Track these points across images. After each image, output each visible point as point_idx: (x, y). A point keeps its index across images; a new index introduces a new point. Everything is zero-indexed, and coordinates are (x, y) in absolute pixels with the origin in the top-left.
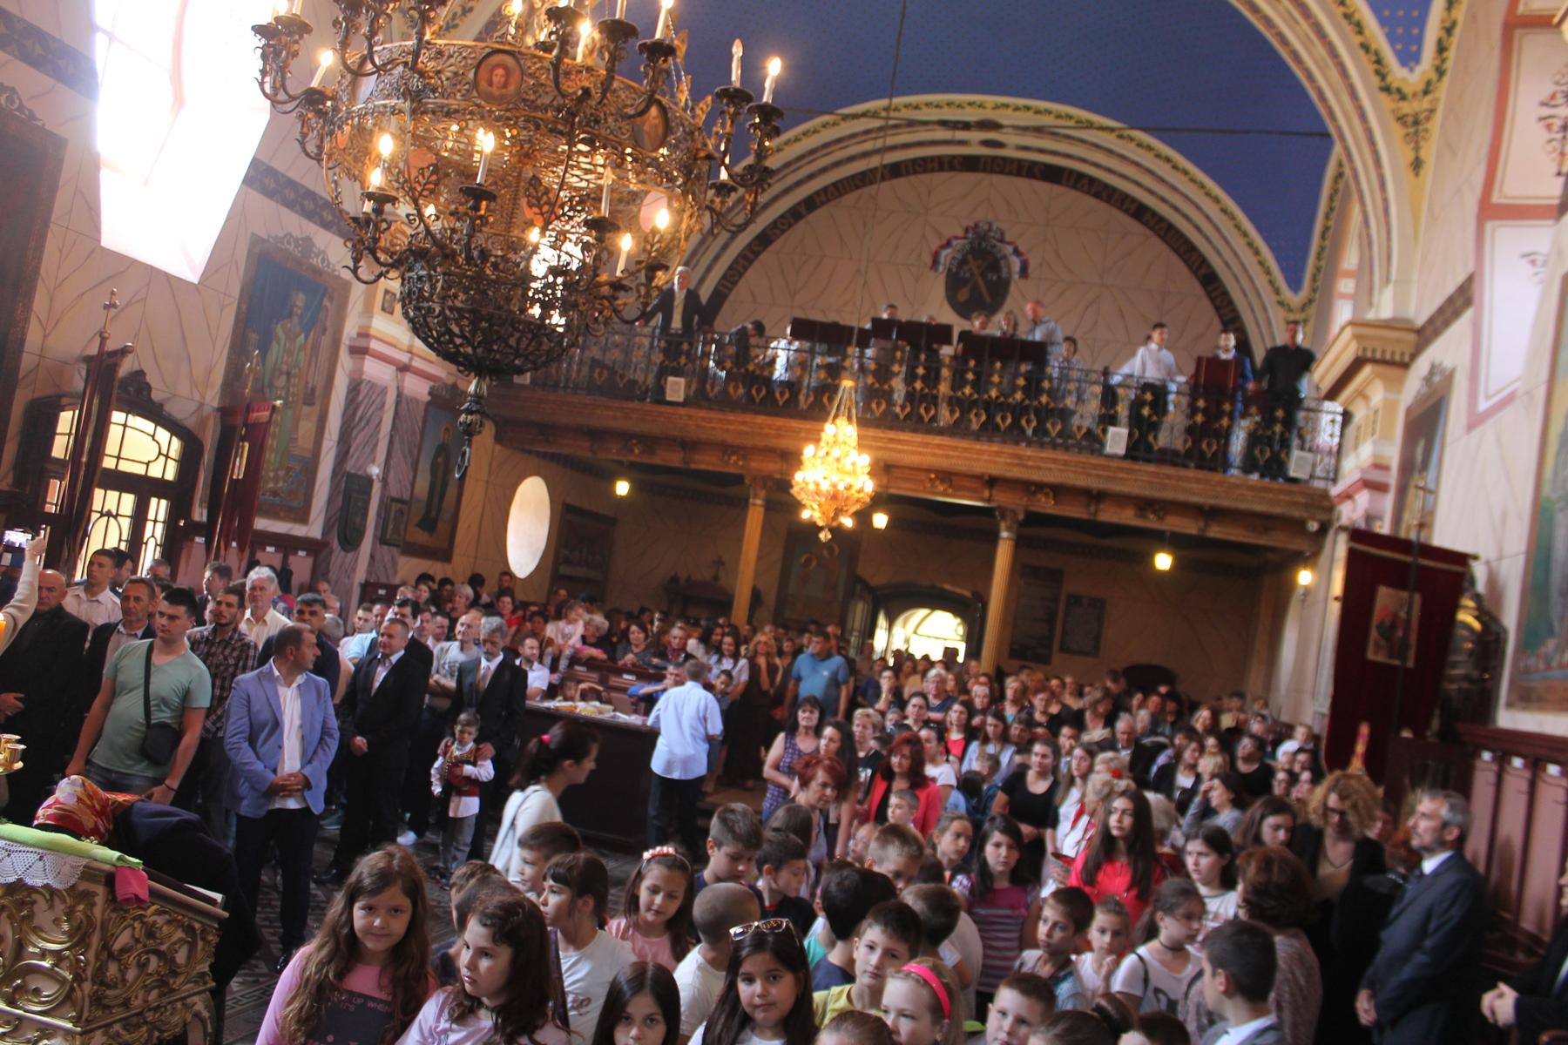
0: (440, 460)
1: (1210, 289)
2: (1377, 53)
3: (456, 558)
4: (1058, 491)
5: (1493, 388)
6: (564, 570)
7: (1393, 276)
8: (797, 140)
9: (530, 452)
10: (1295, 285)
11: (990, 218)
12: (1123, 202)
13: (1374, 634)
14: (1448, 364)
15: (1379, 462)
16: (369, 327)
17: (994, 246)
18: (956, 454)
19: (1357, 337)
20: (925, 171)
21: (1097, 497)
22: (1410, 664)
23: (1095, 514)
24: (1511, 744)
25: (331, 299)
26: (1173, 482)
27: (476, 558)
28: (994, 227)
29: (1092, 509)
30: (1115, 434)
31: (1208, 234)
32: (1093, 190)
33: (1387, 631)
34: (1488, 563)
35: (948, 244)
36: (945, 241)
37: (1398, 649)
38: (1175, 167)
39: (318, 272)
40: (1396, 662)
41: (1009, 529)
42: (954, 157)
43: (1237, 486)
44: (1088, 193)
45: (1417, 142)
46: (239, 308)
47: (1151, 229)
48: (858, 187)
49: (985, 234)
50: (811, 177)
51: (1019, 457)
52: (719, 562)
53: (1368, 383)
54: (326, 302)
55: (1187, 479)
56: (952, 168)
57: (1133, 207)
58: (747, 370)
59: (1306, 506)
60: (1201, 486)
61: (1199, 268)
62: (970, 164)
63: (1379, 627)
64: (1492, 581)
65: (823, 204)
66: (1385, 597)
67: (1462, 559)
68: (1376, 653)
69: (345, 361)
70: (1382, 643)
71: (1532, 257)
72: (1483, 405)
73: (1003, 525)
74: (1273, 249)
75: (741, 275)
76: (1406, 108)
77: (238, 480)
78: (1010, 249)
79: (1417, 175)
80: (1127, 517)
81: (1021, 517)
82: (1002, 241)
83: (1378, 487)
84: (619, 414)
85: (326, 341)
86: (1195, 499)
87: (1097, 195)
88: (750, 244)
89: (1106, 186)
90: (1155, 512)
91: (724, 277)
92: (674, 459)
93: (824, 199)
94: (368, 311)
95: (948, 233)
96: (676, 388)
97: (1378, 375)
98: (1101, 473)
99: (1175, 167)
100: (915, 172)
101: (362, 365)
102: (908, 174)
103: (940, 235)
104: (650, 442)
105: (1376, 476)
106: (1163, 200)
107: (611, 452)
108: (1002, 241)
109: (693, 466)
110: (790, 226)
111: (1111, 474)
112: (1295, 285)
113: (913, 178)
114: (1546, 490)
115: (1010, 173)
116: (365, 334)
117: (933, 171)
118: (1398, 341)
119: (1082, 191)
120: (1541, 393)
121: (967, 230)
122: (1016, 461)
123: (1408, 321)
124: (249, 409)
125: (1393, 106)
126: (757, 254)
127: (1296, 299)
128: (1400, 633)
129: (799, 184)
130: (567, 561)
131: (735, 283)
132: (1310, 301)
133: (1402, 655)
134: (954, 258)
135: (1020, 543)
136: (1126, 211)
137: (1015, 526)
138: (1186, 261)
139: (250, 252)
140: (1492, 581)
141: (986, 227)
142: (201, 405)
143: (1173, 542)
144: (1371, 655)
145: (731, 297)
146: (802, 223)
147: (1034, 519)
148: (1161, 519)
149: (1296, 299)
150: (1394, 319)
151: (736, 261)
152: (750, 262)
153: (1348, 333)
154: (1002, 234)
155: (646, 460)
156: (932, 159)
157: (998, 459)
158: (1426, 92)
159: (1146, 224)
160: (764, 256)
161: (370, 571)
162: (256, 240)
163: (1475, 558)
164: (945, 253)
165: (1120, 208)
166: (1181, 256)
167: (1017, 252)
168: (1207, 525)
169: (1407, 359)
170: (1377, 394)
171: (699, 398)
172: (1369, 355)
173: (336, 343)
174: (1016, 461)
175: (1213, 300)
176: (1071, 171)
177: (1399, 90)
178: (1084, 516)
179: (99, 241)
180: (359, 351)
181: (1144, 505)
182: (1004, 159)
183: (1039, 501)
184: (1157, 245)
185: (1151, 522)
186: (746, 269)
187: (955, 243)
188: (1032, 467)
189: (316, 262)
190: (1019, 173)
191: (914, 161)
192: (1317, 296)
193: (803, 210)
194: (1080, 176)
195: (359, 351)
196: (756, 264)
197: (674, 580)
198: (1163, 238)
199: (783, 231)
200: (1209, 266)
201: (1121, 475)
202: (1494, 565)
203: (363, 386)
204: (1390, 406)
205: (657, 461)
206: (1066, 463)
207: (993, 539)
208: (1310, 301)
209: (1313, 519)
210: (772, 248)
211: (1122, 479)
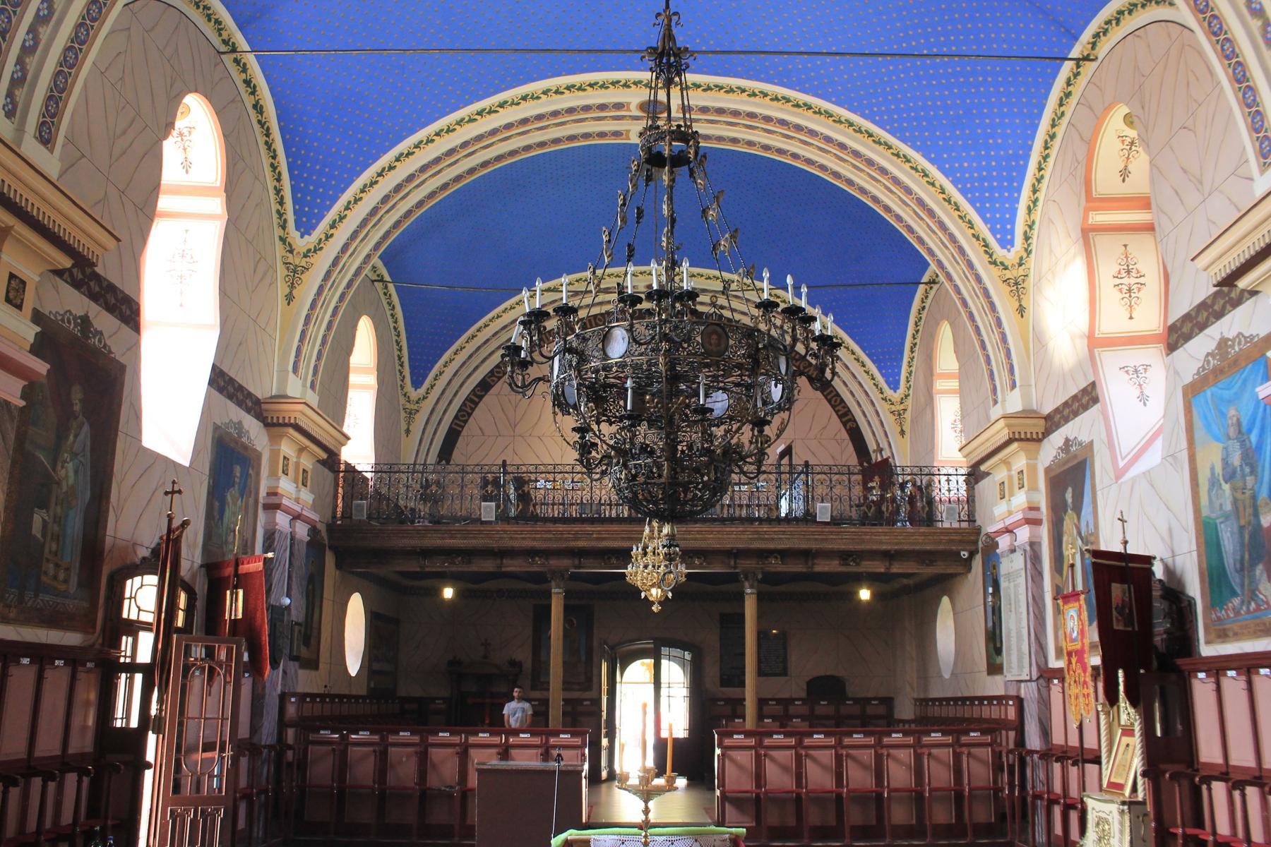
0: (310, 587)
1: (825, 393)
2: (984, 240)
3: (321, 666)
4: (784, 554)
5: (1124, 452)
6: (376, 666)
7: (1018, 384)
9: (353, 573)
10: (894, 386)
13: (1114, 613)
14: (1084, 438)
15: (1032, 506)
16: (278, 487)
18: (711, 536)
19: (1008, 426)
21: (806, 555)
22: (1136, 629)
23: (812, 568)
24: (1217, 667)
25: (253, 468)
26: (868, 537)
29: (810, 563)
30: (822, 508)
33: (1120, 610)
34: (1162, 560)
37: (1128, 621)
39: (245, 447)
40: (1130, 629)
41: (751, 587)
43: (913, 534)
45: (1019, 296)
46: (209, 482)
51: (757, 533)
53: (1013, 454)
54: (251, 471)
55: (878, 534)
58: (523, 491)
59: (961, 542)
63: (1116, 609)
64: (1169, 571)
66: (1117, 590)
67: (1148, 560)
68: (1118, 625)
69: (262, 516)
70: (1120, 618)
71: (1126, 369)
72: (1121, 464)
73: (747, 584)
74: (874, 362)
75: (470, 415)
76: (1008, 274)
77: (236, 620)
79: (1022, 316)
80: (833, 566)
81: (760, 576)
83: (1035, 522)
84: (446, 535)
85: (251, 500)
86: (884, 547)
88: (855, 421)
90: (854, 560)
91: (456, 417)
92: (488, 565)
94: (273, 474)
96: (488, 511)
97: (1022, 449)
101: (275, 518)
104: (469, 554)
105: (1032, 515)
109: (503, 569)
111: (824, 537)
112: (894, 386)
114: (1205, 512)
116: (273, 493)
118: (1034, 425)
120: (1184, 456)
122: (756, 536)
123: (1035, 412)
124: (237, 563)
125: (1000, 273)
126: (481, 398)
127: (896, 396)
128: (1127, 611)
131: (466, 422)
132: (906, 396)
133: (1133, 625)
135: (761, 598)
137: (756, 584)
139: (213, 438)
140: (1169, 571)
142: (193, 562)
144: (1116, 627)
145: (464, 433)
147: (771, 579)
148: (858, 564)
149: (896, 396)
150: (1023, 411)
151: (464, 404)
152: (476, 404)
153: (1002, 423)
155: (466, 569)
157: (742, 536)
158: (1020, 265)
160: (486, 398)
161: (284, 685)
162: (216, 428)
163: (1154, 558)
168: (891, 564)
169: (1040, 436)
170: (1020, 462)
171: (503, 517)
172: (1017, 436)
173: (256, 501)
174: (756, 536)
175: (829, 401)
177: (1002, 263)
178: (804, 570)
179: (140, 441)
180: (272, 507)
181: (845, 556)
185: (852, 568)
186: (473, 410)
188: (767, 539)
189: (244, 440)
192: (911, 392)
195: (272, 507)
196: (481, 404)
201: (832, 537)
202: (1170, 561)
203: (277, 536)
204: (1032, 469)
205: (474, 568)
206: (792, 533)
207: (740, 597)
209: (963, 550)
210: (493, 391)
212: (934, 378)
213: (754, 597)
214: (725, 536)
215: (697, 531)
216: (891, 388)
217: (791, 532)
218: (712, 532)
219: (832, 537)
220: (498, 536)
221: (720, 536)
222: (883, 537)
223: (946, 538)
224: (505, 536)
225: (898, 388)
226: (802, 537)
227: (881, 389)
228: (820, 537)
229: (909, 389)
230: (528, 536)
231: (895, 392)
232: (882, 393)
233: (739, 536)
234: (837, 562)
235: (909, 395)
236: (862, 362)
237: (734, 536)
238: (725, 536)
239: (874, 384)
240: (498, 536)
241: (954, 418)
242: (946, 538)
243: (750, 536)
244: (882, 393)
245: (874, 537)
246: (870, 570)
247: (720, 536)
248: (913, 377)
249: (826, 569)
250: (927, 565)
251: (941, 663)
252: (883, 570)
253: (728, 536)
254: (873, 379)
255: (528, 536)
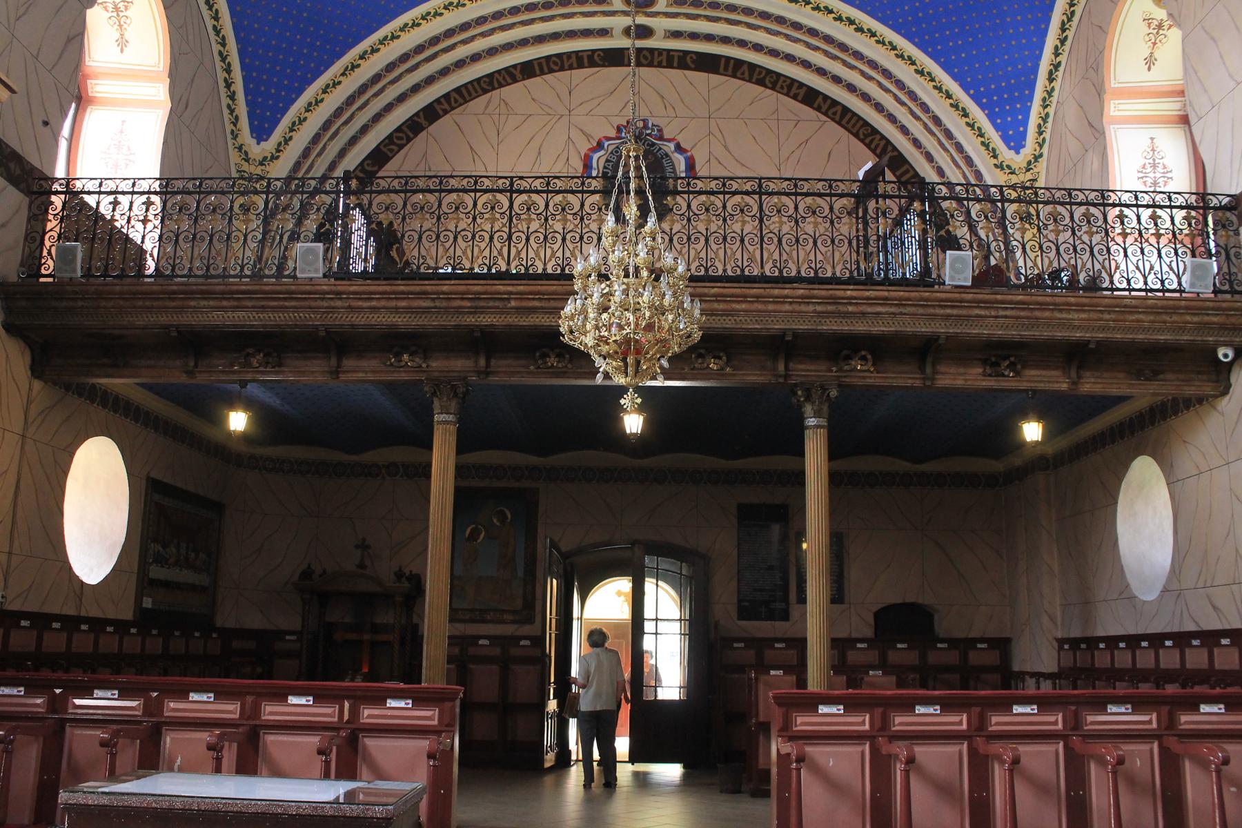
6: (156, 572)
8: (415, 25)
10: (1016, 143)
11: (644, 113)
12: (790, 87)
17: (653, 144)
18: (744, 306)
20: (562, 69)
23: (933, 379)
26: (1047, 314)
27: (10, 553)
28: (650, 125)
29: (929, 370)
31: (892, 111)
32: (755, 77)
35: (600, 146)
36: (595, 144)
38: (860, 30)
41: (817, 414)
42: (594, 51)
44: (750, 81)
47: (826, 114)
48: (485, 92)
49: (641, 133)
50: (430, 80)
52: (363, 546)
56: (593, 64)
57: (802, 92)
59: (1223, 328)
60: (1083, 316)
61: (884, 151)
62: (614, 58)
65: (446, 112)
73: (808, 409)
78: (672, 146)
82: (661, 138)
87: (760, 83)
89: (769, 72)
90: (1012, 366)
93: (446, 106)
95: (598, 134)
98: (949, 311)
99: (860, 30)
100: (551, 71)
102: (542, 73)
103: (588, 137)
106: (837, 80)
107: (216, 372)
108: (661, 138)
110: (409, 140)
112: (1016, 143)
113: (548, 77)
115: (660, 65)
117: (571, 68)
119: (743, 79)
121: (619, 129)
122: (830, 308)
127: (1018, 160)
129: (416, 89)
130: (160, 560)
132: (1037, 158)
134: (607, 161)
136: (795, 97)
137: (825, 408)
138: (868, 146)
141: (641, 124)
143: (1043, 407)
146: (424, 133)
148: (1017, 374)
149: (1018, 160)
154: (660, 131)
156: (569, 55)
157: (804, 308)
159: (818, 109)
164: (596, 156)
165: (787, 95)
166: (862, 141)
167: (679, 148)
174: (830, 308)
176: (728, 59)
178: (918, 383)
182: (651, 50)
183: (855, 369)
184: (834, 130)
187: (606, 144)
190: (670, 65)
191: (548, 58)
192: (1045, 150)
193: (422, 120)
194: (739, 63)
197: (307, 574)
198: (839, 123)
199: (401, 147)
200: (895, 149)
201: (977, 312)
208: (1037, 158)
209: (1226, 344)
211: (978, 316)
212: (1106, 97)
213: (822, 433)
214: (771, 307)
215: (715, 295)
216: (1010, 148)
217: (900, 299)
218: (745, 296)
219: (977, 312)
220: (325, 304)
221: (760, 307)
222: (1076, 316)
223: (1196, 319)
224: (339, 303)
225: (1024, 146)
226: (921, 311)
227: (994, 150)
228: (955, 312)
229: (1041, 146)
230: (383, 303)
231: (1018, 152)
232: (995, 157)
233: (797, 307)
234: (980, 370)
235: (1041, 155)
236: (964, 109)
237: (787, 307)
238: (771, 307)
239: (983, 143)
240: (325, 304)
241: (1143, 161)
242: (1196, 319)
243: (819, 308)
244: (995, 157)
245: (1058, 315)
246: (1041, 386)
247: (760, 307)
248: (1049, 125)
249: (959, 382)
250: (1147, 379)
251: (1128, 576)
252: (1064, 386)
253: (778, 307)
254: (981, 135)
255: (383, 303)
